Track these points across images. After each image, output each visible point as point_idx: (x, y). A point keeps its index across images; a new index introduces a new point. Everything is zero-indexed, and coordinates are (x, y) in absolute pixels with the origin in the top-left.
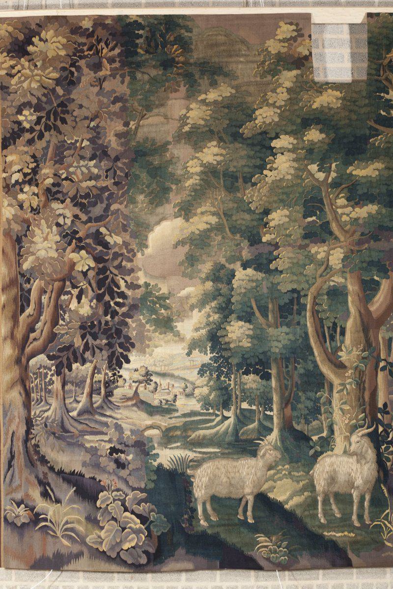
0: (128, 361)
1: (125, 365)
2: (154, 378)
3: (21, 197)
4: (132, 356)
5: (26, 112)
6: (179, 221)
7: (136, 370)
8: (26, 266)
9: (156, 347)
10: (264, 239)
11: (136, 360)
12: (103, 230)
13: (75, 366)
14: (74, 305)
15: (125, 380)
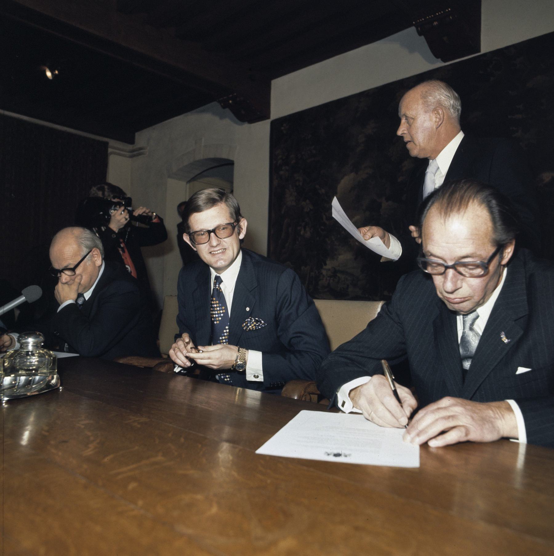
0: (326, 264)
1: (324, 267)
2: (339, 275)
3: (282, 173)
4: (328, 262)
5: (285, 125)
6: (352, 175)
7: (329, 270)
8: (283, 212)
9: (339, 255)
10: (400, 180)
11: (330, 264)
12: (317, 186)
13: (303, 268)
14: (302, 233)
15: (324, 276)
